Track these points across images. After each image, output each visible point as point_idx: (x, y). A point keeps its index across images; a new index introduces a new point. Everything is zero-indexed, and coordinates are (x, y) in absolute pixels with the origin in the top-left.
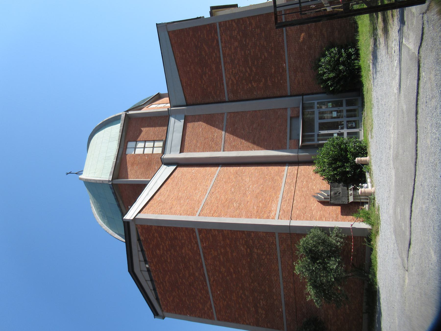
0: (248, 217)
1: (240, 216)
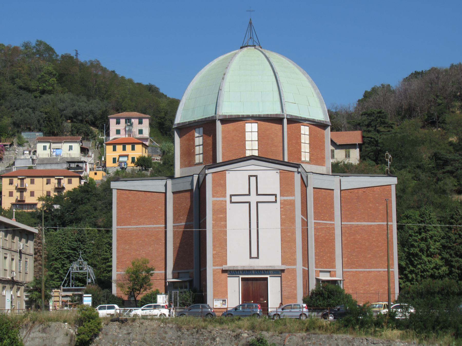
0: (117, 257)
1: (118, 252)
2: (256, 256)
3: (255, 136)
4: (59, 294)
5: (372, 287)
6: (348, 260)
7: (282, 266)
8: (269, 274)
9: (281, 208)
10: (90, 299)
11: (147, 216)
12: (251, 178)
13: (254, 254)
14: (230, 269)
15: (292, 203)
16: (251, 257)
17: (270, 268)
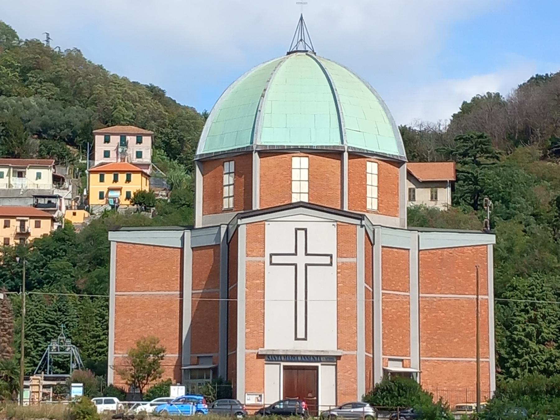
2: (303, 337)
3: (305, 175)
4: (39, 382)
5: (459, 383)
6: (427, 345)
7: (339, 350)
8: (321, 361)
9: (338, 273)
10: (81, 389)
11: (157, 279)
12: (298, 232)
13: (301, 335)
14: (268, 353)
15: (353, 267)
16: (296, 339)
17: (322, 354)
